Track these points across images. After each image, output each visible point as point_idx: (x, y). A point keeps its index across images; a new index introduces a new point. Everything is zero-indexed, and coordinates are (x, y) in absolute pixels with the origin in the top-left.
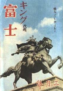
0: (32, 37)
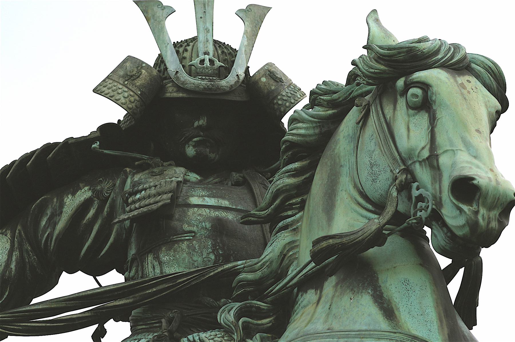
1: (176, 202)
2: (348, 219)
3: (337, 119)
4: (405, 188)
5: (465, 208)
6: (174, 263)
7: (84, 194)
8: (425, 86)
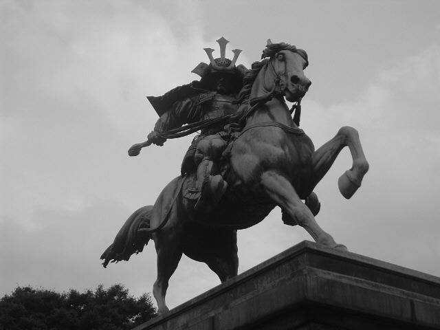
0: (217, 48)
1: (213, 100)
2: (261, 94)
3: (259, 71)
4: (277, 83)
5: (295, 85)
6: (212, 116)
7: (188, 100)
8: (283, 54)
